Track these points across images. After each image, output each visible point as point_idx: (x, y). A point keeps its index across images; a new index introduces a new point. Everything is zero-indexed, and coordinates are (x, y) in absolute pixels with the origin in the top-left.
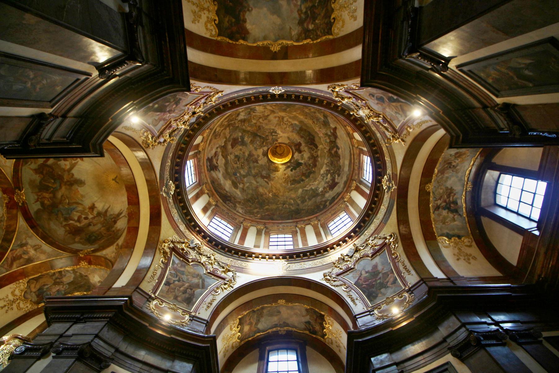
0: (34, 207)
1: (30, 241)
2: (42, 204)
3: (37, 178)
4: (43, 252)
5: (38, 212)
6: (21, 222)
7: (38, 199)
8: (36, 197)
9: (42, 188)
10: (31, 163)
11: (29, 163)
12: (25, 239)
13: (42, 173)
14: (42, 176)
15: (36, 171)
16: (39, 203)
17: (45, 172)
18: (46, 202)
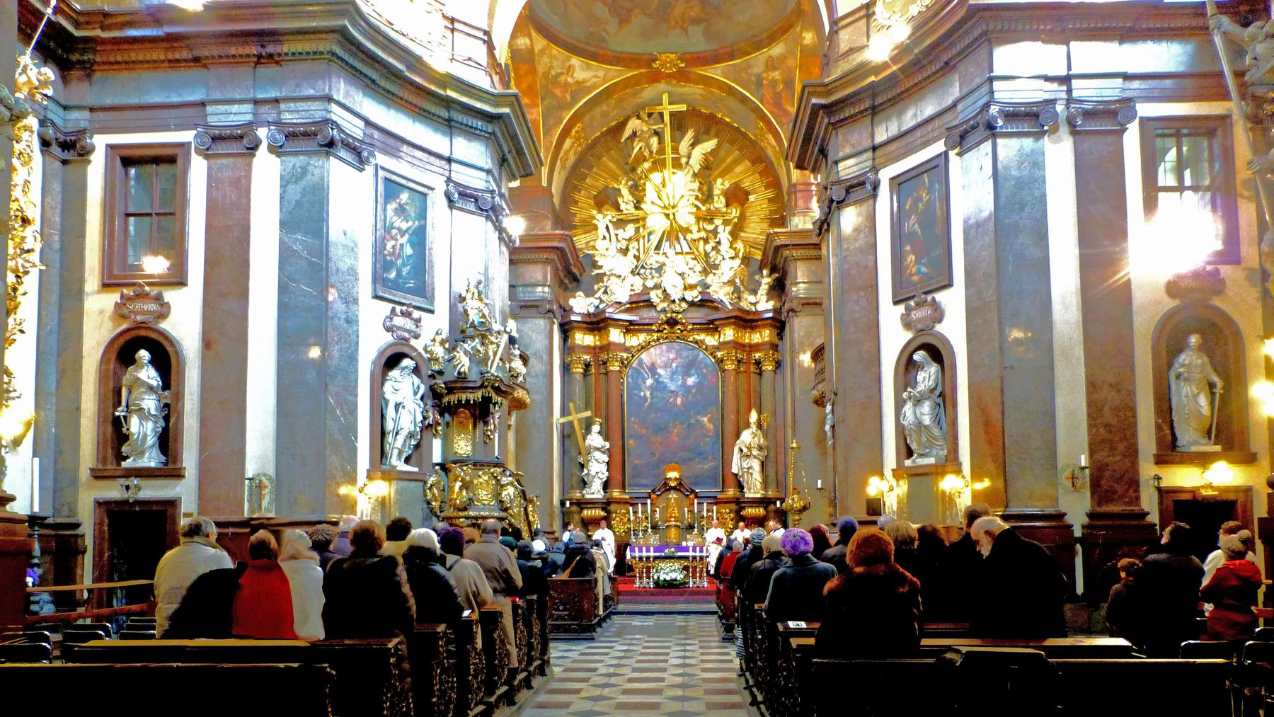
0: (698, 42)
1: (756, 70)
2: (696, 21)
3: (638, 20)
4: (782, 58)
5: (708, 35)
6: (715, 72)
7: (682, 28)
8: (678, 31)
9: (662, 16)
10: (605, 30)
11: (605, 34)
12: (750, 75)
13: (629, 11)
14: (637, 11)
15: (623, 21)
16: (691, 29)
17: (629, 5)
18: (693, 14)
